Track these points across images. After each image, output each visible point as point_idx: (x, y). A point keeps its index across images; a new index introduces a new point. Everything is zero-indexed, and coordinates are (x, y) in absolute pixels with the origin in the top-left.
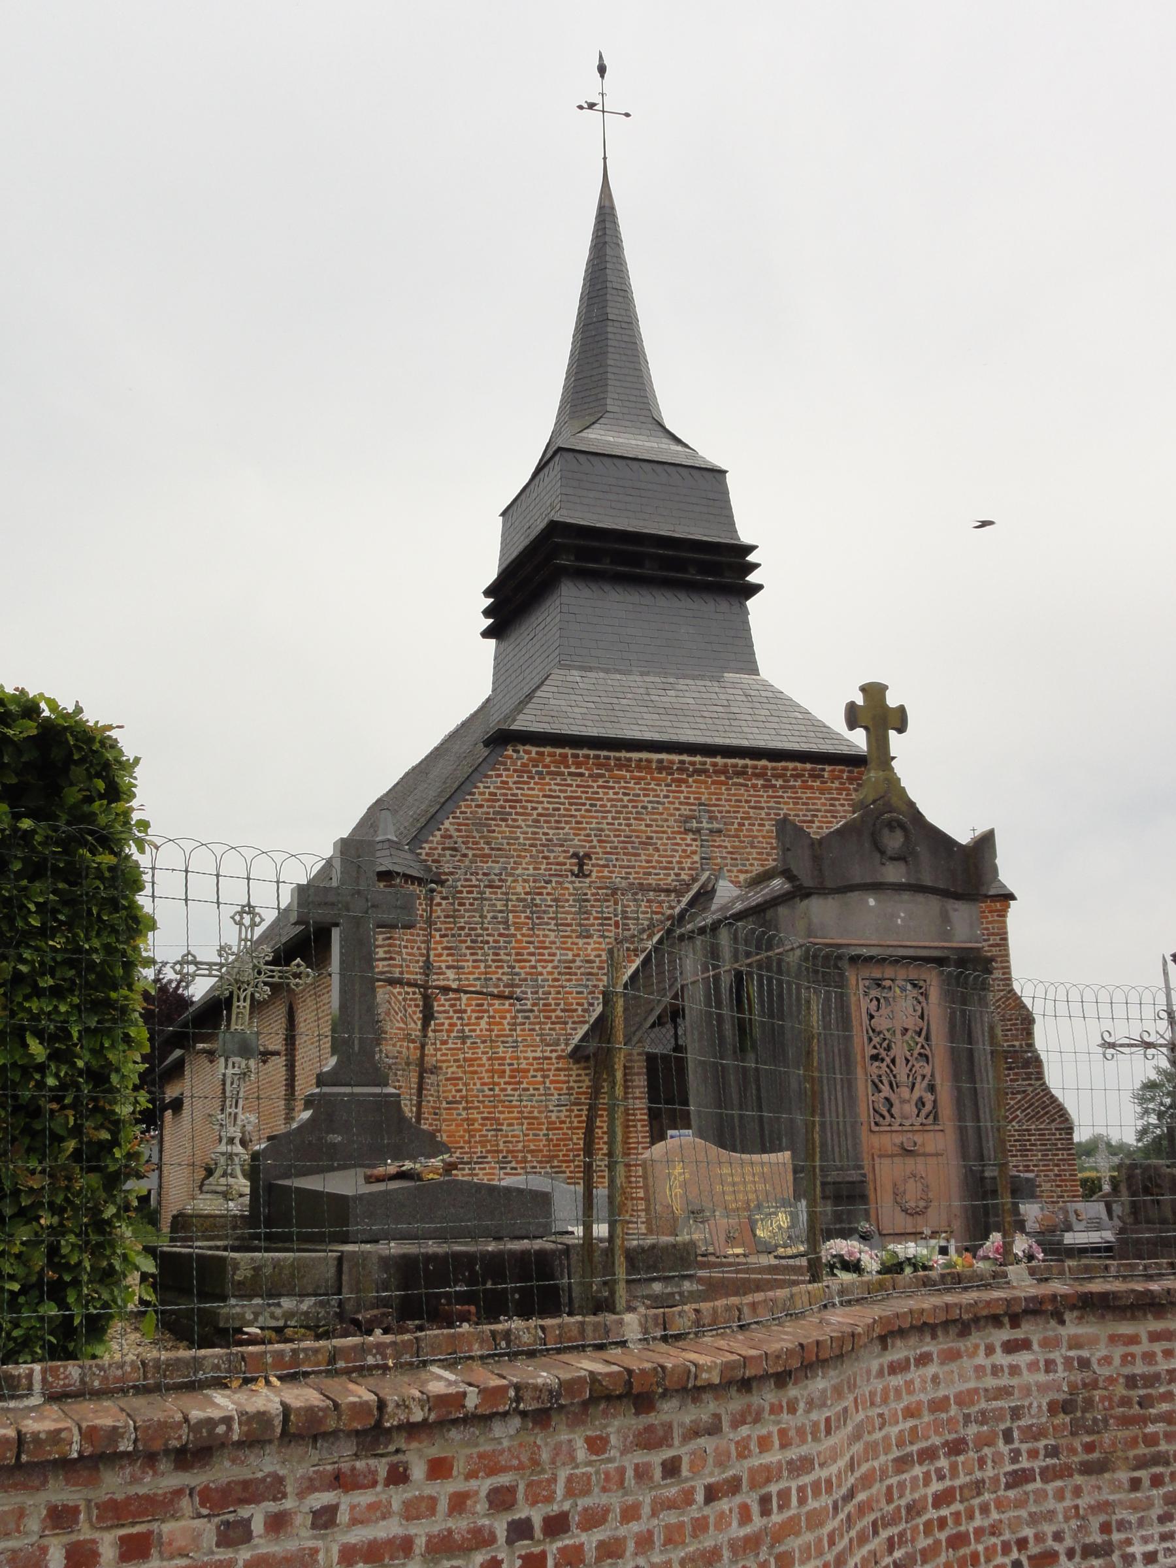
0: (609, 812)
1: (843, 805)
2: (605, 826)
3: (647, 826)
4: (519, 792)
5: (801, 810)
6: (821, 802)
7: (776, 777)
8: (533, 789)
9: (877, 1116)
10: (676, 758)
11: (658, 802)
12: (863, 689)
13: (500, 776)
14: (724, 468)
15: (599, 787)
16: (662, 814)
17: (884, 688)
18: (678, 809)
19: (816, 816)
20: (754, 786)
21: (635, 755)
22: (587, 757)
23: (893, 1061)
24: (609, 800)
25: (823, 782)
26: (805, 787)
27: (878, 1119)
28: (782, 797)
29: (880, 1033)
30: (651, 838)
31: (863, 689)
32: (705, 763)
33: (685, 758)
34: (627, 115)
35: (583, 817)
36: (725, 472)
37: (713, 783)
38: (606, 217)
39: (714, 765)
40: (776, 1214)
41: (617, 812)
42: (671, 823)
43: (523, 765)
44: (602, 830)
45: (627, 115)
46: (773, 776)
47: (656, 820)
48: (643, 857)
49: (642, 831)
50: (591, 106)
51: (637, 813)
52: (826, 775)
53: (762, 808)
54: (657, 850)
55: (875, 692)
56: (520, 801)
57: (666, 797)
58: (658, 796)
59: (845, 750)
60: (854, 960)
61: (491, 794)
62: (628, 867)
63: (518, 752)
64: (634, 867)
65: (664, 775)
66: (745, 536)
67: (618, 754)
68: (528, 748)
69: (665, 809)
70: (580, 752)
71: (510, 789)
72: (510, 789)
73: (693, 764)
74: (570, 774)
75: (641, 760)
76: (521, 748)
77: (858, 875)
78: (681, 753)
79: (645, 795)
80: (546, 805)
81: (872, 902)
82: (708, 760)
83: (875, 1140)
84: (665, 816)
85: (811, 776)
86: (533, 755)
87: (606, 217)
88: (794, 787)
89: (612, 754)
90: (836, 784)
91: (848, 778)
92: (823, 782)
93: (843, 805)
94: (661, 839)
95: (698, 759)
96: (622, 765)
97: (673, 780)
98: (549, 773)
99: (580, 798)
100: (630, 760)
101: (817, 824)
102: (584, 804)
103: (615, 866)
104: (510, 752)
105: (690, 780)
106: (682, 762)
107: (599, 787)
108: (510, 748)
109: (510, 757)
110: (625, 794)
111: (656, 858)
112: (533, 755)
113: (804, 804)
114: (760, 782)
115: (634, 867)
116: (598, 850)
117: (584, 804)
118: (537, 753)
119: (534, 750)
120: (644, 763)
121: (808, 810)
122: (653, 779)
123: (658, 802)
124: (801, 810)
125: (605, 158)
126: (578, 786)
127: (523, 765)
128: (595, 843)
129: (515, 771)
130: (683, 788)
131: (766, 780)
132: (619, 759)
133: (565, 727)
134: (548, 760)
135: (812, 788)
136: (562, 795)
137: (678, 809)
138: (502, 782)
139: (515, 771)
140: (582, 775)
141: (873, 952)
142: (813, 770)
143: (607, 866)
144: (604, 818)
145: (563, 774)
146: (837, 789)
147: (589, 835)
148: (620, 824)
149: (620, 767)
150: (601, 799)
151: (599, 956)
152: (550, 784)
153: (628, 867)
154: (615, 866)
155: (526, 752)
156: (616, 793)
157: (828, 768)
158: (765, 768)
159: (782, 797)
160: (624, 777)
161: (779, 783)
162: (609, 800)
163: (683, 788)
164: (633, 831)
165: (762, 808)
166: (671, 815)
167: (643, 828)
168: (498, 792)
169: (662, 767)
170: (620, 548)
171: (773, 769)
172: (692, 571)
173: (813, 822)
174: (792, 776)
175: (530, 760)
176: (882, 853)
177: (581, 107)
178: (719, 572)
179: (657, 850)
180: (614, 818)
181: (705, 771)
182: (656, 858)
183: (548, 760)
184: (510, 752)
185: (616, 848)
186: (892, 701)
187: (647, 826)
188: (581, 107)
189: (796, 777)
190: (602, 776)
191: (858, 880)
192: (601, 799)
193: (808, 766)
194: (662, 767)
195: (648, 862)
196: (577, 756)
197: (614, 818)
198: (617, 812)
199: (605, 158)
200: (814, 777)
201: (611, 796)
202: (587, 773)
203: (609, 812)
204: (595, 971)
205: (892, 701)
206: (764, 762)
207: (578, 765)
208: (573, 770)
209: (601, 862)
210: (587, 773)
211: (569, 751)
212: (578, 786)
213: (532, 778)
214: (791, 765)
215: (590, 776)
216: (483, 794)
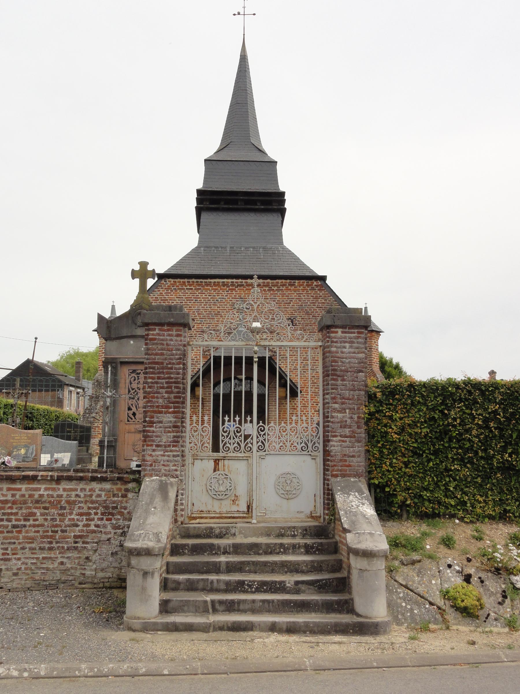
0: (203, 303)
1: (305, 296)
2: (201, 308)
3: (218, 307)
4: (167, 296)
5: (285, 299)
6: (294, 295)
7: (274, 286)
8: (172, 295)
9: (129, 418)
10: (230, 280)
11: (223, 298)
12: (140, 263)
13: (160, 291)
14: (276, 160)
15: (199, 293)
16: (224, 303)
17: (148, 263)
18: (231, 301)
19: (292, 301)
20: (265, 290)
21: (213, 281)
22: (193, 282)
23: (138, 399)
24: (203, 298)
25: (295, 287)
26: (287, 289)
27: (129, 419)
28: (277, 294)
29: (134, 389)
30: (219, 312)
31: (140, 263)
32: (242, 282)
33: (234, 280)
34: (254, 14)
35: (192, 305)
36: (276, 162)
37: (247, 289)
38: (243, 59)
39: (246, 282)
40: (21, 449)
41: (206, 303)
42: (228, 306)
43: (168, 286)
44: (200, 310)
45: (254, 14)
46: (272, 285)
47: (222, 305)
48: (216, 320)
49: (216, 310)
50: (239, 14)
51: (214, 303)
52: (296, 284)
53: (268, 299)
54: (222, 316)
55: (144, 265)
56: (167, 300)
57: (226, 296)
58: (223, 296)
59: (308, 274)
60: (122, 363)
61: (155, 298)
62: (209, 323)
63: (166, 281)
64: (212, 323)
65: (225, 287)
66: (282, 189)
67: (205, 280)
68: (170, 280)
69: (226, 300)
70: (191, 280)
71: (163, 296)
72: (163, 296)
73: (237, 282)
74: (187, 289)
75: (215, 282)
76: (167, 280)
77: (125, 333)
78: (233, 279)
79: (217, 296)
80: (177, 301)
81: (132, 342)
82: (244, 281)
83: (127, 427)
84: (226, 303)
85: (289, 285)
86: (172, 282)
87: (243, 59)
88: (282, 290)
89: (203, 281)
90: (302, 288)
91: (306, 285)
92: (295, 287)
93: (305, 296)
94: (224, 312)
95: (240, 280)
96: (209, 284)
97: (229, 289)
98: (178, 289)
99: (191, 298)
100: (211, 282)
101: (292, 304)
102: (193, 300)
103: (204, 323)
104: (163, 282)
105: (237, 289)
106: (232, 282)
107: (199, 293)
108: (163, 280)
109: (163, 284)
110: (209, 296)
111: (221, 320)
112: (172, 282)
113: (286, 296)
114: (267, 289)
115: (212, 323)
116: (197, 317)
117: (193, 300)
118: (174, 282)
119: (172, 280)
120: (216, 283)
121: (288, 299)
122: (221, 289)
123: (223, 298)
124: (285, 299)
125: (244, 35)
126: (190, 293)
127: (168, 286)
128: (197, 315)
129: (165, 289)
130: (234, 292)
131: (269, 288)
132: (206, 282)
133: (194, 271)
134: (178, 284)
135: (290, 290)
136: (184, 297)
137: (231, 301)
138: (160, 293)
139: (165, 289)
140: (192, 289)
141: (131, 360)
142: (290, 282)
143: (201, 323)
144: (200, 305)
145: (184, 289)
146: (302, 289)
147: (194, 312)
148: (207, 307)
149: (207, 285)
150: (200, 298)
151: (197, 357)
152: (179, 293)
153: (209, 323)
154: (204, 323)
155: (169, 281)
156: (206, 295)
157: (297, 281)
158: (268, 283)
159: (277, 294)
160: (209, 289)
161: (276, 288)
162: (203, 298)
163: (234, 292)
164: (213, 310)
165: (268, 299)
166: (228, 303)
167: (216, 308)
168: (159, 297)
169: (224, 284)
170: (240, 195)
171: (272, 283)
172: (259, 204)
173: (290, 303)
174: (281, 285)
175: (171, 284)
176: (136, 324)
177: (234, 15)
178: (272, 203)
179: (222, 316)
180: (204, 305)
181: (243, 285)
182: (221, 320)
183: (178, 284)
184: (163, 282)
185: (205, 316)
186: (137, 268)
187: (218, 307)
188: (234, 15)
189: (283, 286)
190: (200, 289)
191: (125, 335)
192: (200, 298)
193: (288, 281)
194: (224, 284)
195: (217, 321)
196: (189, 282)
197: (204, 305)
198: (206, 303)
199: (244, 35)
200: (291, 285)
201: (204, 296)
202: (194, 288)
203: (203, 303)
204: (194, 363)
205: (137, 268)
206: (269, 281)
207: (190, 285)
208: (188, 287)
209: (198, 322)
210: (194, 288)
211: (186, 280)
212: (190, 293)
213: (172, 291)
214: (280, 281)
215: (195, 289)
216: (153, 298)
